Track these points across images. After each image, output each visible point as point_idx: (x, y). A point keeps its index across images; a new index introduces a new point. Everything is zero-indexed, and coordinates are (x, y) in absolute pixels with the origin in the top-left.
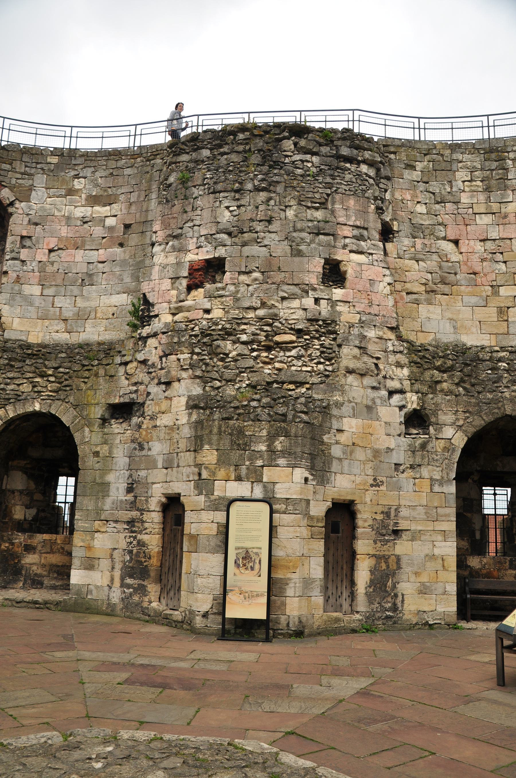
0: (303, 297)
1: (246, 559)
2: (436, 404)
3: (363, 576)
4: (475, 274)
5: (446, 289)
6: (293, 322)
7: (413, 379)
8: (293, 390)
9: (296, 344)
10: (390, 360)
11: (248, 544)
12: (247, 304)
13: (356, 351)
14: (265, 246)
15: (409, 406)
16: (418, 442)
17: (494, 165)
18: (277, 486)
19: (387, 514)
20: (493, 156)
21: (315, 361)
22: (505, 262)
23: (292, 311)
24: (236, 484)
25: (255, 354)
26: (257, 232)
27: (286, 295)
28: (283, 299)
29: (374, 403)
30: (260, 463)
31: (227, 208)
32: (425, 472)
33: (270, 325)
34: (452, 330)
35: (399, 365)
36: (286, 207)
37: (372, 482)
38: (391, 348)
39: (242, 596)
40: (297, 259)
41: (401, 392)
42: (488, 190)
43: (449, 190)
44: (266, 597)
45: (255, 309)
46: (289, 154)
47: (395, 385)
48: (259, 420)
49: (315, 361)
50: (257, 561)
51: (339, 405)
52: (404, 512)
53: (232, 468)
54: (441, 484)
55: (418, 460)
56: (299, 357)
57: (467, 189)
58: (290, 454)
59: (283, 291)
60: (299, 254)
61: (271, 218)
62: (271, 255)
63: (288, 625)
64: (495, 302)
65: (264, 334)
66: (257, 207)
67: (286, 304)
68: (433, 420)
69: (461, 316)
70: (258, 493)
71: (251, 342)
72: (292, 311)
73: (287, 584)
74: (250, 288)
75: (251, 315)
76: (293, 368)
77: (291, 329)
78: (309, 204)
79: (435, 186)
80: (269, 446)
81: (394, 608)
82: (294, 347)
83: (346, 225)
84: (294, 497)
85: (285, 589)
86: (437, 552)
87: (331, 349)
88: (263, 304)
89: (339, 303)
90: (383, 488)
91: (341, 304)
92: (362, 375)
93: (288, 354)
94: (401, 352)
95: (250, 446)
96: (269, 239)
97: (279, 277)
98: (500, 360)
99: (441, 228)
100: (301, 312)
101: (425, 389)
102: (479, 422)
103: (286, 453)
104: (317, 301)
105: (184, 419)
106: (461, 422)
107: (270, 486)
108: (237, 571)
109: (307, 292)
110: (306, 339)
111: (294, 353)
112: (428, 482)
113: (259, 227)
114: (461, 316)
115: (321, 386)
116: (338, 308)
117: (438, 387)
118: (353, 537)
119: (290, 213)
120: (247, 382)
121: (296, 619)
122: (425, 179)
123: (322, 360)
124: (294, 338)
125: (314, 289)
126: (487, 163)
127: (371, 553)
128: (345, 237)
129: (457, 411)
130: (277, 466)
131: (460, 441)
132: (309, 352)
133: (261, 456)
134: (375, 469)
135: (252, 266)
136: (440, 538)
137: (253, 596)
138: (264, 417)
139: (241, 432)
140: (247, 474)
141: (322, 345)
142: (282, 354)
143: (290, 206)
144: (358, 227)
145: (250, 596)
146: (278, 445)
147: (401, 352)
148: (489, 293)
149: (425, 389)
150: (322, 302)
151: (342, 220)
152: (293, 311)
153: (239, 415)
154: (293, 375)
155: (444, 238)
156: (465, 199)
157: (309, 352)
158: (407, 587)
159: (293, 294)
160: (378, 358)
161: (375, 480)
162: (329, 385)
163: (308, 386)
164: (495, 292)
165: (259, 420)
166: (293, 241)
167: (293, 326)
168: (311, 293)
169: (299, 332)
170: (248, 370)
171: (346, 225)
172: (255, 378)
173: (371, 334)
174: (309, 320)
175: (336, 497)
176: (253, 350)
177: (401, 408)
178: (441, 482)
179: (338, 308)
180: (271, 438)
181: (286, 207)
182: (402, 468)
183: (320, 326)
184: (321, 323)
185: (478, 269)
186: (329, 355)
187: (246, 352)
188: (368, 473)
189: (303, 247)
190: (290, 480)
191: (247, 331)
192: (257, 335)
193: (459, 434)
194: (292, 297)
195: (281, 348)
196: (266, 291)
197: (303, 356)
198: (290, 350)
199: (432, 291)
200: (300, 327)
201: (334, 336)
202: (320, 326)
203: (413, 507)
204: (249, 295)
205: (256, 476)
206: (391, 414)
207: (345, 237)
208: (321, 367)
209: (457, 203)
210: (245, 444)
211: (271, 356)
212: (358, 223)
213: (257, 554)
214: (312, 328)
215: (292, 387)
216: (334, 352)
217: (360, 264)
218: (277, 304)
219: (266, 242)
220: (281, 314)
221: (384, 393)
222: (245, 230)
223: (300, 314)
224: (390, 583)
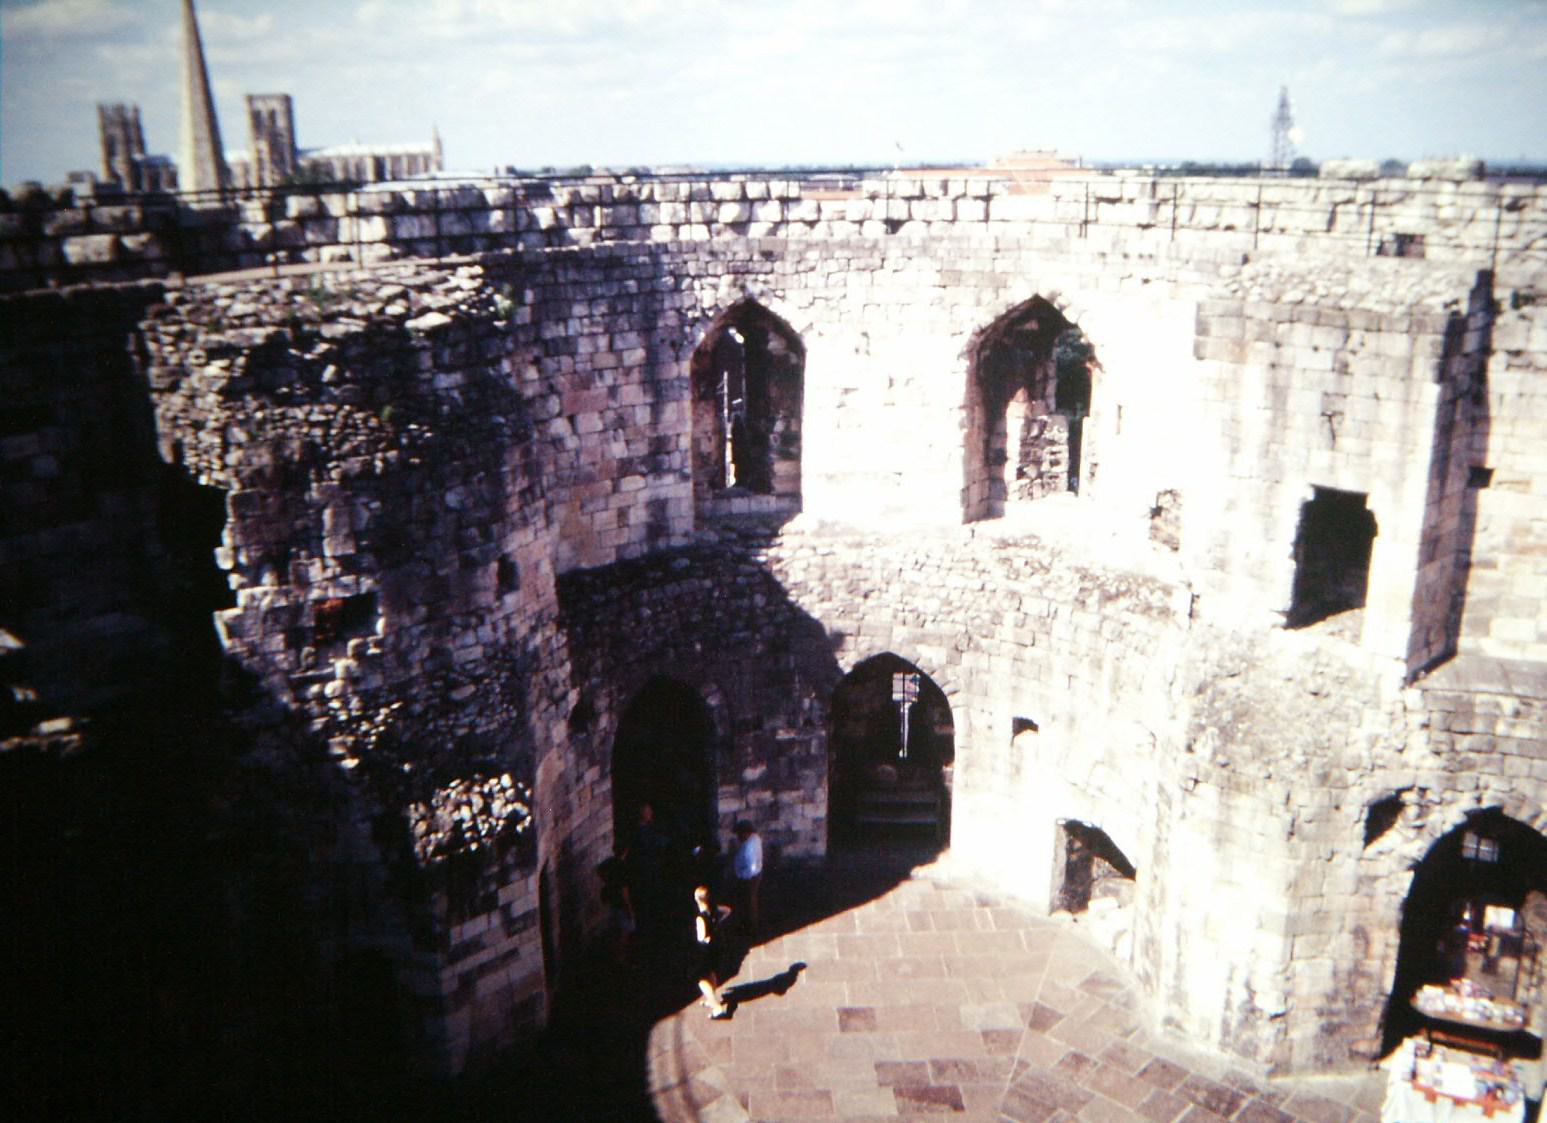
25: (431, 726)
31: (366, 505)
35: (562, 663)
46: (427, 376)
64: (615, 502)
67: (458, 643)
71: (425, 712)
93: (468, 711)
104: (495, 628)
105: (374, 855)
111: (472, 709)
124: (472, 689)
141: (502, 686)
152: (469, 648)
164: (616, 489)
168: (488, 619)
173: (538, 639)
179: (514, 623)
189: (475, 552)
206: (560, 731)
209: (573, 354)
221: (553, 708)
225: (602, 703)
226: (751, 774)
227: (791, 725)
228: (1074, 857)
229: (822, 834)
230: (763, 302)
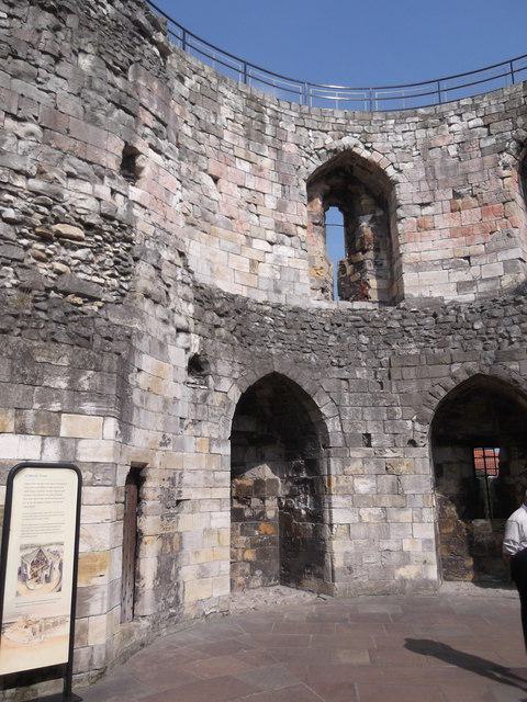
0: (95, 182)
1: (39, 563)
2: (216, 351)
3: (148, 565)
4: (232, 218)
5: (206, 226)
6: (84, 212)
7: (198, 319)
8: (80, 305)
9: (84, 244)
10: (179, 291)
11: (41, 539)
12: (18, 165)
13: (153, 272)
14: (48, 92)
15: (192, 348)
16: (199, 394)
17: (255, 114)
18: (82, 444)
19: (172, 480)
20: (254, 104)
21: (108, 272)
22: (258, 215)
23: (82, 196)
24: (16, 438)
25: (25, 242)
26: (37, 66)
27: (73, 171)
28: (70, 175)
29: (166, 339)
30: (56, 407)
32: (205, 429)
33: (49, 207)
34: (209, 273)
35: (186, 300)
36: (80, 50)
37: (161, 439)
38: (179, 277)
39: (29, 631)
40: (92, 128)
41: (187, 331)
42: (247, 136)
43: (213, 121)
44: (68, 625)
45: (28, 176)
47: (181, 321)
48: (54, 341)
49: (108, 272)
50: (56, 566)
51: (140, 335)
52: (187, 478)
53: (11, 413)
54: (219, 445)
55: (200, 416)
56: (88, 262)
57: (229, 128)
58: (100, 395)
59: (72, 165)
60: (95, 121)
61: (61, 55)
62: (56, 108)
63: (90, 663)
64: (249, 253)
65: (41, 217)
66: (39, 31)
68: (213, 368)
69: (217, 259)
70: (52, 453)
72: (82, 196)
73: (91, 596)
74: (21, 143)
75: (20, 182)
76: (80, 275)
77: (79, 220)
78: (111, 63)
79: (201, 111)
80: (71, 382)
81: (177, 602)
82: (83, 247)
83: (147, 109)
84: (105, 460)
85: (88, 605)
86: (214, 524)
87: (126, 260)
88: (41, 173)
89: (136, 206)
90: (170, 448)
91: (139, 208)
92: (156, 302)
93: (72, 254)
94: (189, 284)
95: (42, 379)
96: (53, 83)
97: (67, 144)
98: (265, 313)
99: (204, 158)
100: (94, 202)
101: (206, 333)
102: (253, 378)
103: (96, 395)
104: (113, 192)
106: (236, 375)
107: (71, 444)
108: (22, 587)
109: (102, 178)
110: (97, 240)
111: (80, 253)
112: (206, 442)
113: (42, 60)
114: (217, 259)
115: (119, 307)
116: (135, 211)
117: (217, 331)
118: (139, 513)
119: (85, 62)
120: (15, 282)
121: (103, 652)
122: (193, 100)
123: (117, 274)
124: (80, 233)
125: (112, 177)
126: (249, 110)
127: (159, 532)
128: (146, 125)
129: (233, 362)
130: (82, 413)
131: (235, 396)
132: (101, 258)
133: (59, 397)
134: (165, 422)
135: (28, 112)
136: (216, 507)
137: (47, 627)
138: (63, 338)
139: (27, 356)
140: (35, 423)
142: (63, 251)
143: (86, 53)
144: (158, 119)
145: (38, 628)
146: (85, 382)
147: (189, 284)
148: (243, 242)
149: (206, 333)
150: (118, 196)
151: (145, 101)
152: (83, 197)
153: (22, 328)
154: (81, 285)
155: (205, 171)
156: (227, 136)
157: (101, 258)
158: (187, 573)
159: (85, 174)
160: (169, 286)
161: (164, 436)
162: (128, 308)
163: (100, 304)
164: (249, 245)
165: (54, 341)
166: (86, 102)
167: (82, 217)
168: (107, 180)
169: (89, 227)
170: (16, 264)
171: (147, 109)
172: (27, 279)
174: (103, 216)
175: (135, 460)
176: (23, 236)
177: (187, 350)
178: (219, 442)
180: (75, 371)
181: (80, 50)
182: (186, 422)
183: (115, 227)
184: (116, 223)
185: (235, 215)
186: (123, 268)
187: (12, 235)
188: (159, 428)
189: (100, 115)
190: (95, 435)
191: (15, 205)
192: (30, 215)
193: (235, 388)
194: (85, 178)
195: (62, 244)
196: (47, 156)
197: (92, 262)
198: (74, 249)
199: (193, 225)
200: (93, 221)
201: (128, 245)
202: (115, 227)
203: (193, 471)
204: (20, 152)
205: (48, 427)
207: (146, 125)
208: (114, 281)
210: (36, 377)
211: (48, 251)
212: (159, 115)
213: (56, 554)
214: (105, 227)
215: (79, 300)
216: (130, 265)
217: (158, 166)
218: (61, 180)
219: (49, 86)
220: (66, 196)
221: (173, 330)
222: (20, 55)
223: (91, 204)
224: (173, 571)
225: (223, 367)
226: (363, 486)
230: (355, 150)
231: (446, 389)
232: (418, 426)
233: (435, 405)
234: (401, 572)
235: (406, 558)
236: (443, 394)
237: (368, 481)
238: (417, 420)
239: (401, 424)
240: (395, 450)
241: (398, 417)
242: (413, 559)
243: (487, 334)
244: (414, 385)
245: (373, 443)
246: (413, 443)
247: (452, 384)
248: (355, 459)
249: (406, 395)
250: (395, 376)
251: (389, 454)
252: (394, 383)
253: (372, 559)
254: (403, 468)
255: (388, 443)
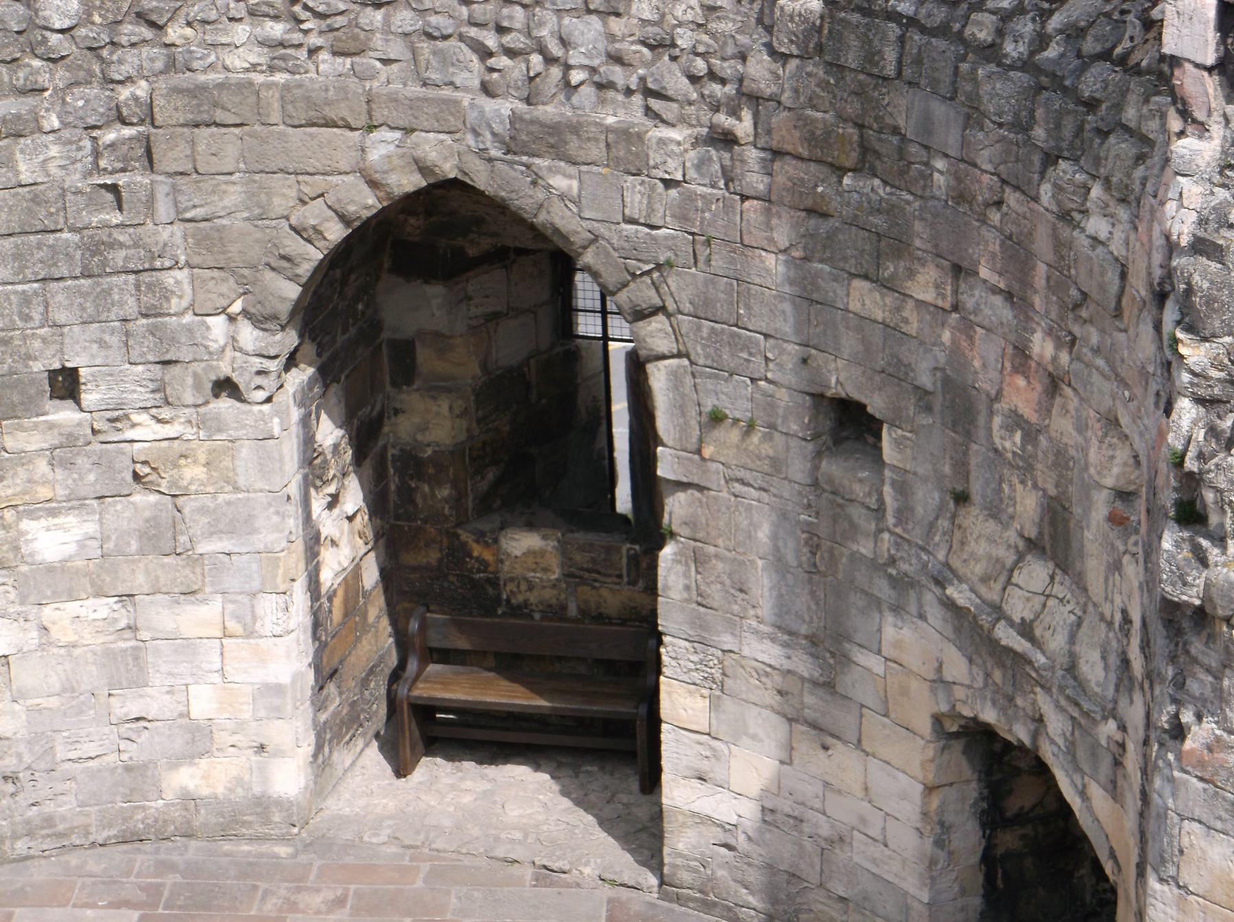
227: (164, 397)
228: (1009, 840)
229: (294, 734)
231: (344, 219)
232: (248, 335)
233: (305, 270)
234: (186, 778)
235: (198, 740)
236: (336, 232)
237: (70, 520)
238: (245, 312)
239: (189, 330)
240: (165, 413)
241: (175, 304)
242: (222, 738)
243: (501, 30)
244: (233, 196)
245: (89, 398)
246: (226, 387)
247: (366, 203)
248: (23, 458)
249: (207, 237)
250: (171, 157)
251: (146, 430)
252: (162, 191)
253: (94, 742)
254: (193, 473)
255: (141, 395)
